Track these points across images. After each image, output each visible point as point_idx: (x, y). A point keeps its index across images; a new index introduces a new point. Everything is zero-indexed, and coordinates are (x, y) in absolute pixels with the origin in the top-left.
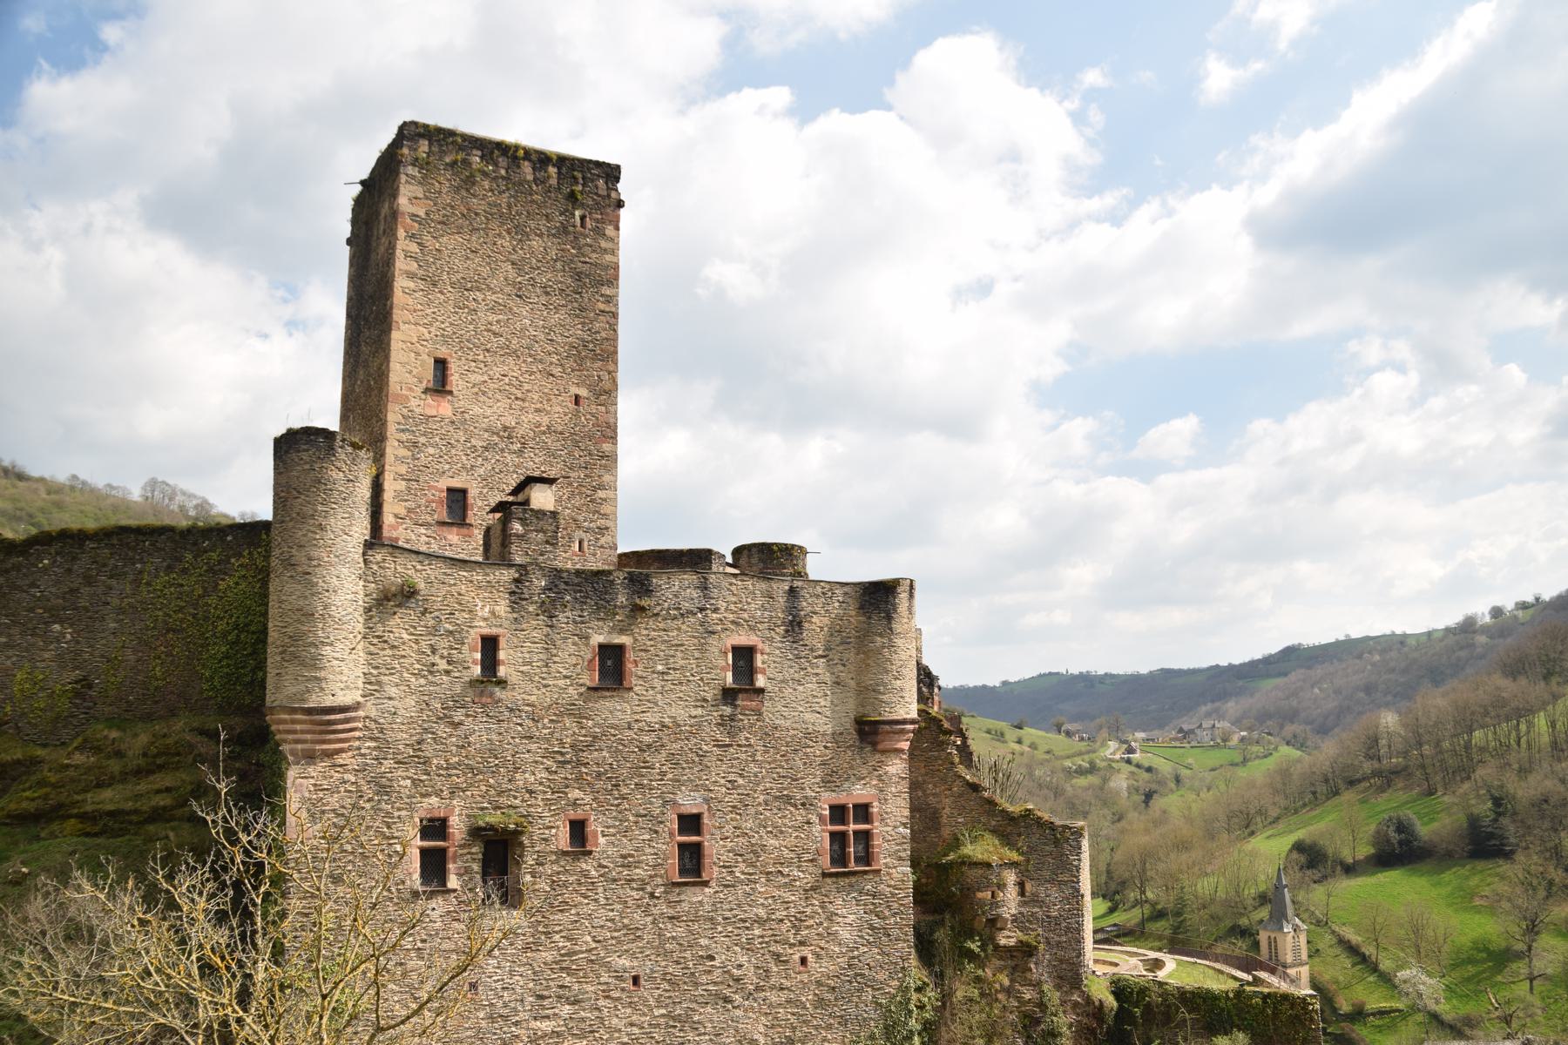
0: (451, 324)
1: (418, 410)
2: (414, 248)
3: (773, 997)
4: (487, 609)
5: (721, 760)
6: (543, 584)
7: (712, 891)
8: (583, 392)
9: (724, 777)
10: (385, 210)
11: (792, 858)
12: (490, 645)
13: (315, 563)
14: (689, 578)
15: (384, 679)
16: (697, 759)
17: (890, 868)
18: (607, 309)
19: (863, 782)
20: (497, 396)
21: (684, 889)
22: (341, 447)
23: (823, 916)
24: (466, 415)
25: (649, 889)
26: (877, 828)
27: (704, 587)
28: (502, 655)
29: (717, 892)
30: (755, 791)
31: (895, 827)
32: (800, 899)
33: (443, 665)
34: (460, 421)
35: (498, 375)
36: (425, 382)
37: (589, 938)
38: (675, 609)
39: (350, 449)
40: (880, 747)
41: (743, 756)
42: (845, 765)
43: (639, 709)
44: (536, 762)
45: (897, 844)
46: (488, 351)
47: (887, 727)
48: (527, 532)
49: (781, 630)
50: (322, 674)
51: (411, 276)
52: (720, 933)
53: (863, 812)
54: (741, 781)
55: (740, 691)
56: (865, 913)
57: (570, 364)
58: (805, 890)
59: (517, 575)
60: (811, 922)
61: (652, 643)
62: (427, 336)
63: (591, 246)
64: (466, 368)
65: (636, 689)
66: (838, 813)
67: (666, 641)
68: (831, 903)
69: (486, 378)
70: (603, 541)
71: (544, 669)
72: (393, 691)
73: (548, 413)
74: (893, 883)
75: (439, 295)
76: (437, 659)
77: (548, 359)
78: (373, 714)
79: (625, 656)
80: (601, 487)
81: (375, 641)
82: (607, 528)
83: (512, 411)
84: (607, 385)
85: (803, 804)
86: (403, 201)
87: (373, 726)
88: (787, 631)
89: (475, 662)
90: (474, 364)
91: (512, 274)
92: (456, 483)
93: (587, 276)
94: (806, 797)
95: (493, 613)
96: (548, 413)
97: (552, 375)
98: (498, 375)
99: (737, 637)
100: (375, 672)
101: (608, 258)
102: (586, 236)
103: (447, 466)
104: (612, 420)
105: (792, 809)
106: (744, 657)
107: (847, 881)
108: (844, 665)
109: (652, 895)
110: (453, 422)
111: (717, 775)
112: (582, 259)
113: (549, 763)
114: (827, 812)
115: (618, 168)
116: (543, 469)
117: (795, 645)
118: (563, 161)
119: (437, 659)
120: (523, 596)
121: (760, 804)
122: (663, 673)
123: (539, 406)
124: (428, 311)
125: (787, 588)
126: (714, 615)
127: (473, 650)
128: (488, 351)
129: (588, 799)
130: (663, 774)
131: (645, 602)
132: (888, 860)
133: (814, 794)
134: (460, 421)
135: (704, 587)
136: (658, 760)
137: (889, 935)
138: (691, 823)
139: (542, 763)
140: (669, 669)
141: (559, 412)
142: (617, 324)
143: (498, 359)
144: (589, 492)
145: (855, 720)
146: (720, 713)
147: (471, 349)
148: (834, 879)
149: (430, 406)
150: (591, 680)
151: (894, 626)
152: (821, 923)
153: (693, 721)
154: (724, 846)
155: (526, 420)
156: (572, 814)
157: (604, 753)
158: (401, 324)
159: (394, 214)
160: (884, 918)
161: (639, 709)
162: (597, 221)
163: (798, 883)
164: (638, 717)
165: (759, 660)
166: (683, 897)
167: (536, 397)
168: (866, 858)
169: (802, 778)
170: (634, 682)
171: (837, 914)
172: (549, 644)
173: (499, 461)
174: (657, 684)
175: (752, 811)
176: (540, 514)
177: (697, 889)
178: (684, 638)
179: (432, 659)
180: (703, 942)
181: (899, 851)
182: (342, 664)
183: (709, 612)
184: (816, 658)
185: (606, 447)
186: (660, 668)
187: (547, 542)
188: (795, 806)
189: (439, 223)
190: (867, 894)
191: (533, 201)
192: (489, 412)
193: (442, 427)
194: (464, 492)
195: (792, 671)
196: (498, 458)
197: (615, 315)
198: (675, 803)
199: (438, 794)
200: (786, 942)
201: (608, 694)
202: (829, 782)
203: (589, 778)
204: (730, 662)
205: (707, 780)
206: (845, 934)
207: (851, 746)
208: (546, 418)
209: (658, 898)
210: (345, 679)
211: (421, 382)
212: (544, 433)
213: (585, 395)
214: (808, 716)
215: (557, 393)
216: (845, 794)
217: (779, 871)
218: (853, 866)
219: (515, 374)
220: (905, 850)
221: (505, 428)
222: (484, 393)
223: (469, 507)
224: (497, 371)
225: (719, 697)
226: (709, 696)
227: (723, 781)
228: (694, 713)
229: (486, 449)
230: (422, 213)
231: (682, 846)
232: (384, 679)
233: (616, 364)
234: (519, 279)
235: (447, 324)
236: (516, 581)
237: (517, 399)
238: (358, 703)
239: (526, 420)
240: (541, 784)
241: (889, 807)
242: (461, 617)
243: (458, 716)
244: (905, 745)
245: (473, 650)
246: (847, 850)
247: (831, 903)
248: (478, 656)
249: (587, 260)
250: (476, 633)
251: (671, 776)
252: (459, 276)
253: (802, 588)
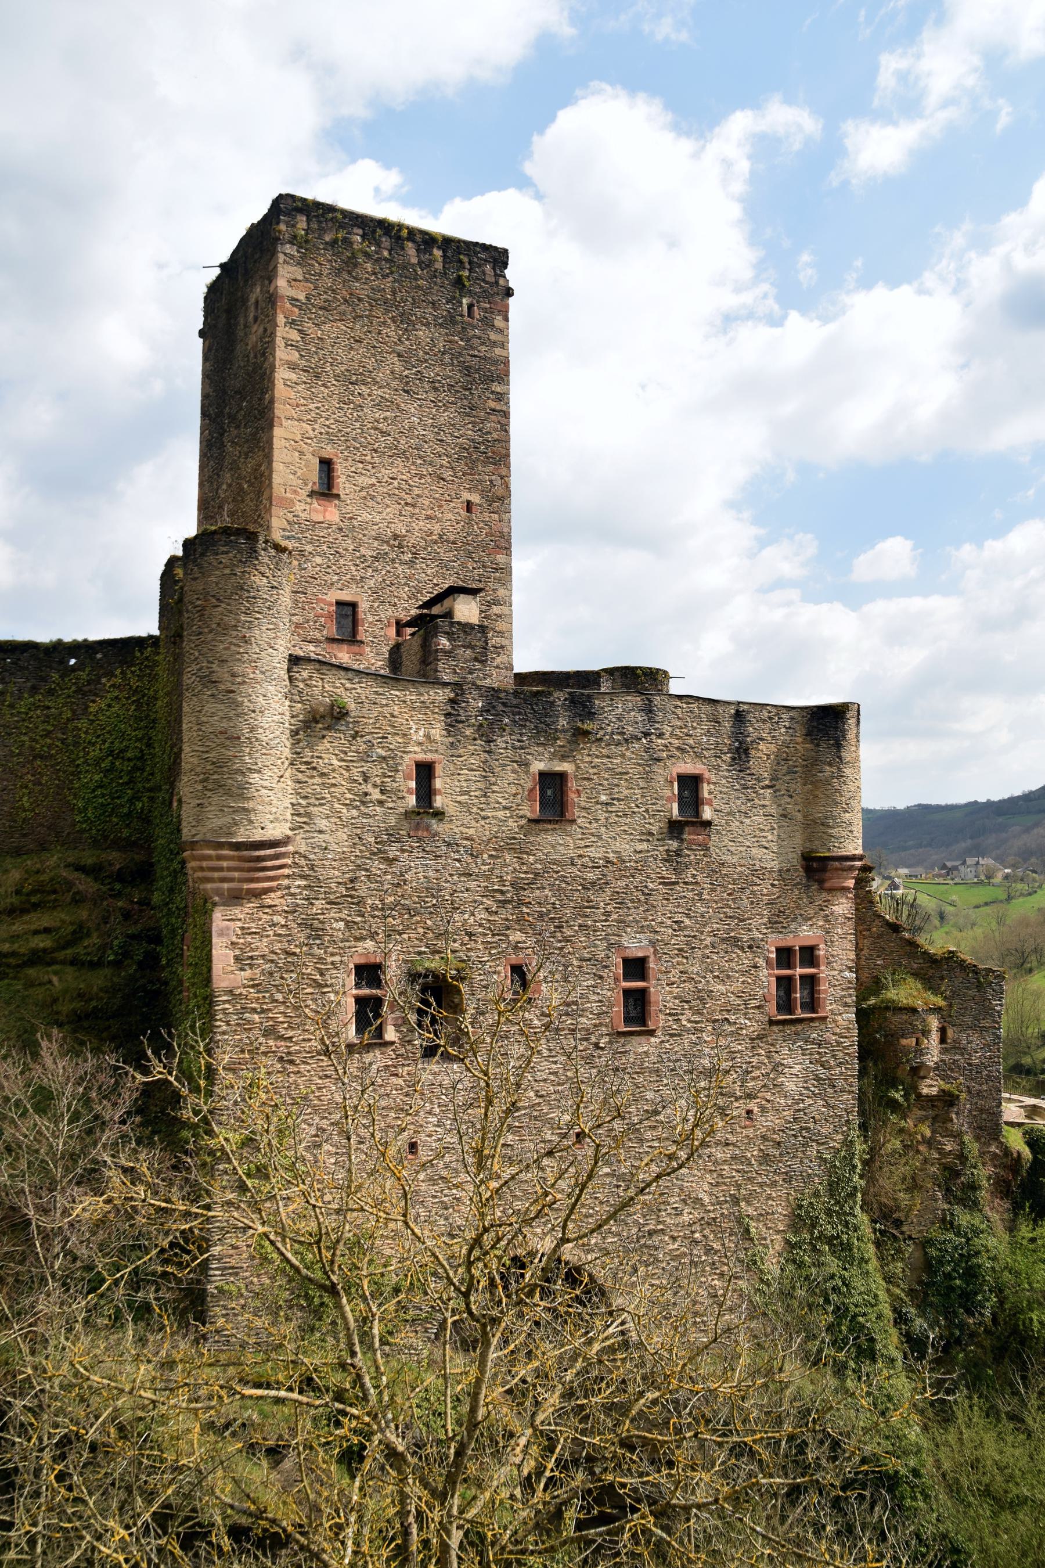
0: (337, 421)
1: (303, 515)
2: (295, 335)
3: (719, 1154)
4: (421, 733)
6: (480, 704)
7: (658, 1040)
8: (475, 498)
9: (670, 918)
10: (256, 293)
11: (739, 1005)
12: (425, 772)
13: (239, 680)
14: (634, 700)
15: (314, 810)
16: (642, 898)
17: (835, 1015)
18: (498, 408)
19: (810, 923)
20: (387, 501)
21: (629, 1038)
22: (264, 550)
23: (770, 1067)
24: (355, 522)
25: (593, 1039)
26: (824, 972)
27: (648, 710)
28: (438, 784)
29: (663, 1042)
30: (702, 933)
31: (841, 971)
32: (747, 1048)
33: (376, 794)
34: (348, 528)
35: (386, 479)
36: (310, 485)
37: (532, 1094)
38: (618, 733)
39: (273, 552)
40: (827, 885)
41: (690, 895)
42: (792, 905)
43: (582, 843)
45: (843, 989)
46: (375, 451)
47: (837, 864)
49: (727, 757)
50: (250, 805)
51: (293, 367)
52: (666, 1085)
53: (809, 955)
55: (687, 823)
56: (811, 1063)
57: (460, 467)
58: (751, 1039)
59: (452, 695)
60: (757, 1073)
61: (595, 771)
62: (311, 434)
63: (479, 338)
64: (353, 469)
65: (579, 821)
66: (785, 956)
67: (609, 769)
68: (777, 1052)
69: (374, 481)
71: (483, 800)
72: (323, 824)
73: (439, 520)
74: (838, 1031)
75: (322, 388)
76: (369, 788)
77: (438, 461)
78: (303, 849)
79: (566, 785)
80: (496, 602)
81: (303, 768)
82: (502, 647)
83: (402, 518)
84: (499, 491)
85: (750, 947)
86: (281, 283)
87: (303, 862)
89: (409, 792)
90: (361, 466)
91: (398, 367)
92: (346, 596)
93: (477, 371)
94: (753, 939)
95: (427, 736)
96: (439, 520)
97: (442, 479)
98: (386, 479)
99: (683, 764)
100: (303, 802)
101: (498, 351)
102: (475, 327)
103: (336, 578)
104: (505, 530)
105: (739, 952)
106: (690, 784)
107: (793, 1028)
109: (597, 1046)
110: (340, 529)
111: (663, 915)
112: (471, 352)
113: (489, 902)
114: (774, 956)
115: (505, 252)
116: (435, 581)
118: (448, 243)
119: (369, 788)
120: (459, 718)
121: (706, 947)
122: (607, 804)
123: (429, 512)
124: (312, 406)
125: (733, 711)
126: (659, 741)
127: (407, 777)
128: (375, 451)
129: (531, 941)
130: (607, 914)
131: (588, 726)
132: (834, 1006)
133: (761, 936)
134: (348, 528)
135: (648, 710)
136: (602, 899)
137: (834, 1086)
138: (636, 967)
140: (613, 799)
141: (451, 517)
142: (508, 425)
143: (387, 460)
145: (803, 855)
146: (666, 848)
147: (358, 448)
148: (781, 1027)
149: (316, 511)
150: (532, 811)
151: (843, 754)
152: (768, 1074)
153: (638, 856)
154: (670, 992)
155: (417, 528)
156: (514, 959)
157: (547, 892)
159: (272, 299)
160: (830, 1068)
161: (582, 843)
162: (485, 310)
163: (744, 1031)
164: (580, 852)
165: (706, 790)
166: (627, 1048)
167: (427, 503)
168: (812, 1004)
169: (749, 919)
170: (577, 814)
171: (783, 1065)
172: (487, 772)
173: (389, 572)
174: (601, 815)
175: (698, 954)
176: (466, 628)
177: (642, 1039)
178: (628, 766)
179: (364, 788)
180: (650, 1095)
181: (844, 996)
182: (271, 793)
183: (653, 737)
185: (500, 558)
186: (604, 798)
187: (476, 659)
188: (742, 949)
189: (321, 308)
190: (813, 1043)
191: (418, 287)
192: (378, 519)
193: (329, 535)
194: (353, 606)
195: (739, 802)
196: (388, 568)
197: (506, 415)
198: (620, 946)
199: (373, 936)
200: (732, 1095)
201: (549, 827)
203: (531, 919)
204: (676, 792)
205: (653, 920)
206: (791, 1086)
207: (798, 884)
208: (437, 526)
209: (602, 1049)
210: (274, 810)
212: (436, 542)
213: (477, 501)
215: (448, 498)
216: (791, 935)
217: (726, 1019)
218: (800, 1014)
219: (404, 477)
220: (851, 996)
221: (395, 536)
222: (373, 498)
223: (360, 623)
224: (385, 473)
226: (655, 829)
228: (639, 847)
229: (376, 558)
230: (302, 297)
231: (627, 992)
232: (314, 810)
233: (509, 468)
234: (406, 373)
235: (332, 421)
236: (452, 701)
237: (407, 504)
238: (288, 837)
239: (417, 528)
240: (480, 925)
241: (836, 950)
242: (395, 741)
243: (393, 851)
244: (851, 883)
245: (407, 777)
246: (793, 995)
247: (777, 1052)
248: (413, 784)
249: (476, 353)
252: (343, 368)
253: (749, 712)
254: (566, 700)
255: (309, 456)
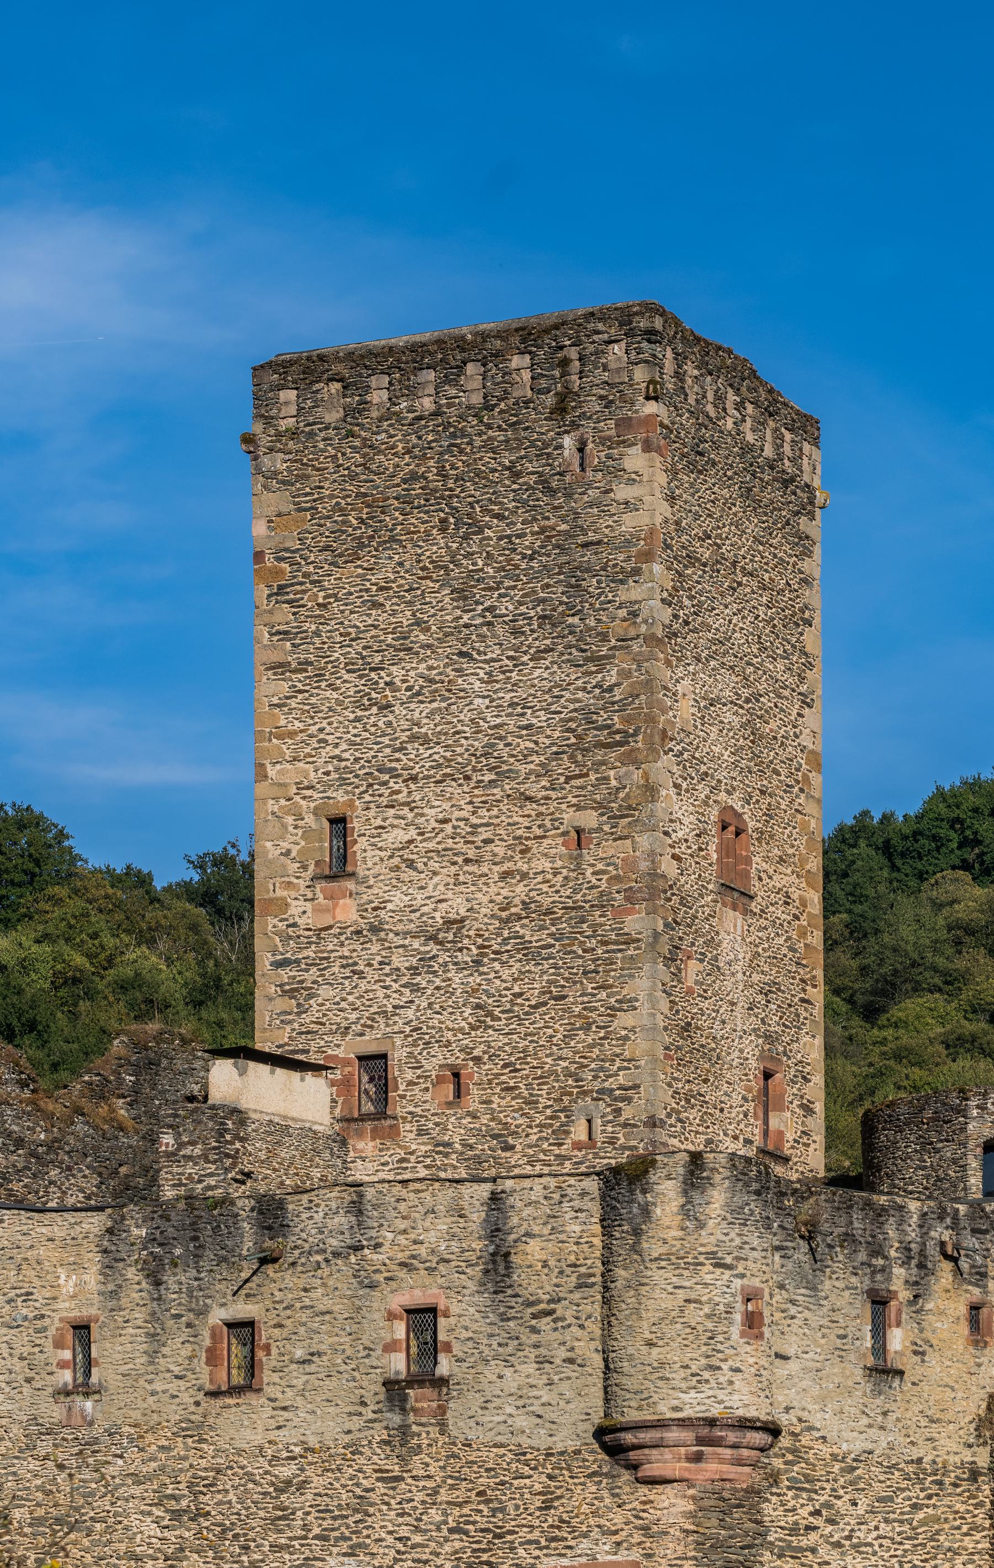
5: (387, 1504)
8: (589, 819)
36: (312, 868)
44: (142, 1513)
46: (414, 778)
48: (181, 1145)
54: (417, 1539)
59: (109, 1224)
64: (379, 822)
69: (413, 833)
70: (628, 1113)
71: (151, 1368)
77: (523, 769)
88: (486, 1272)
89: (62, 1365)
90: (391, 812)
97: (529, 799)
108: (581, 1327)
116: (517, 989)
117: (500, 1297)
120: (118, 1256)
123: (507, 866)
128: (414, 778)
139: (150, 1514)
143: (431, 790)
144: (601, 1021)
155: (485, 900)
158: (269, 767)
184: (534, 1316)
196: (438, 982)
202: (555, 1539)
208: (520, 888)
211: (305, 868)
214: (522, 1422)
215: (539, 832)
225: (382, 1397)
227: (390, 1540)
229: (414, 970)
234: (466, 618)
236: (110, 1231)
237: (467, 861)
245: (59, 1344)
248: (67, 1355)
250: (61, 1320)
251: (317, 1531)
254: (252, 1210)
255: (310, 820)
